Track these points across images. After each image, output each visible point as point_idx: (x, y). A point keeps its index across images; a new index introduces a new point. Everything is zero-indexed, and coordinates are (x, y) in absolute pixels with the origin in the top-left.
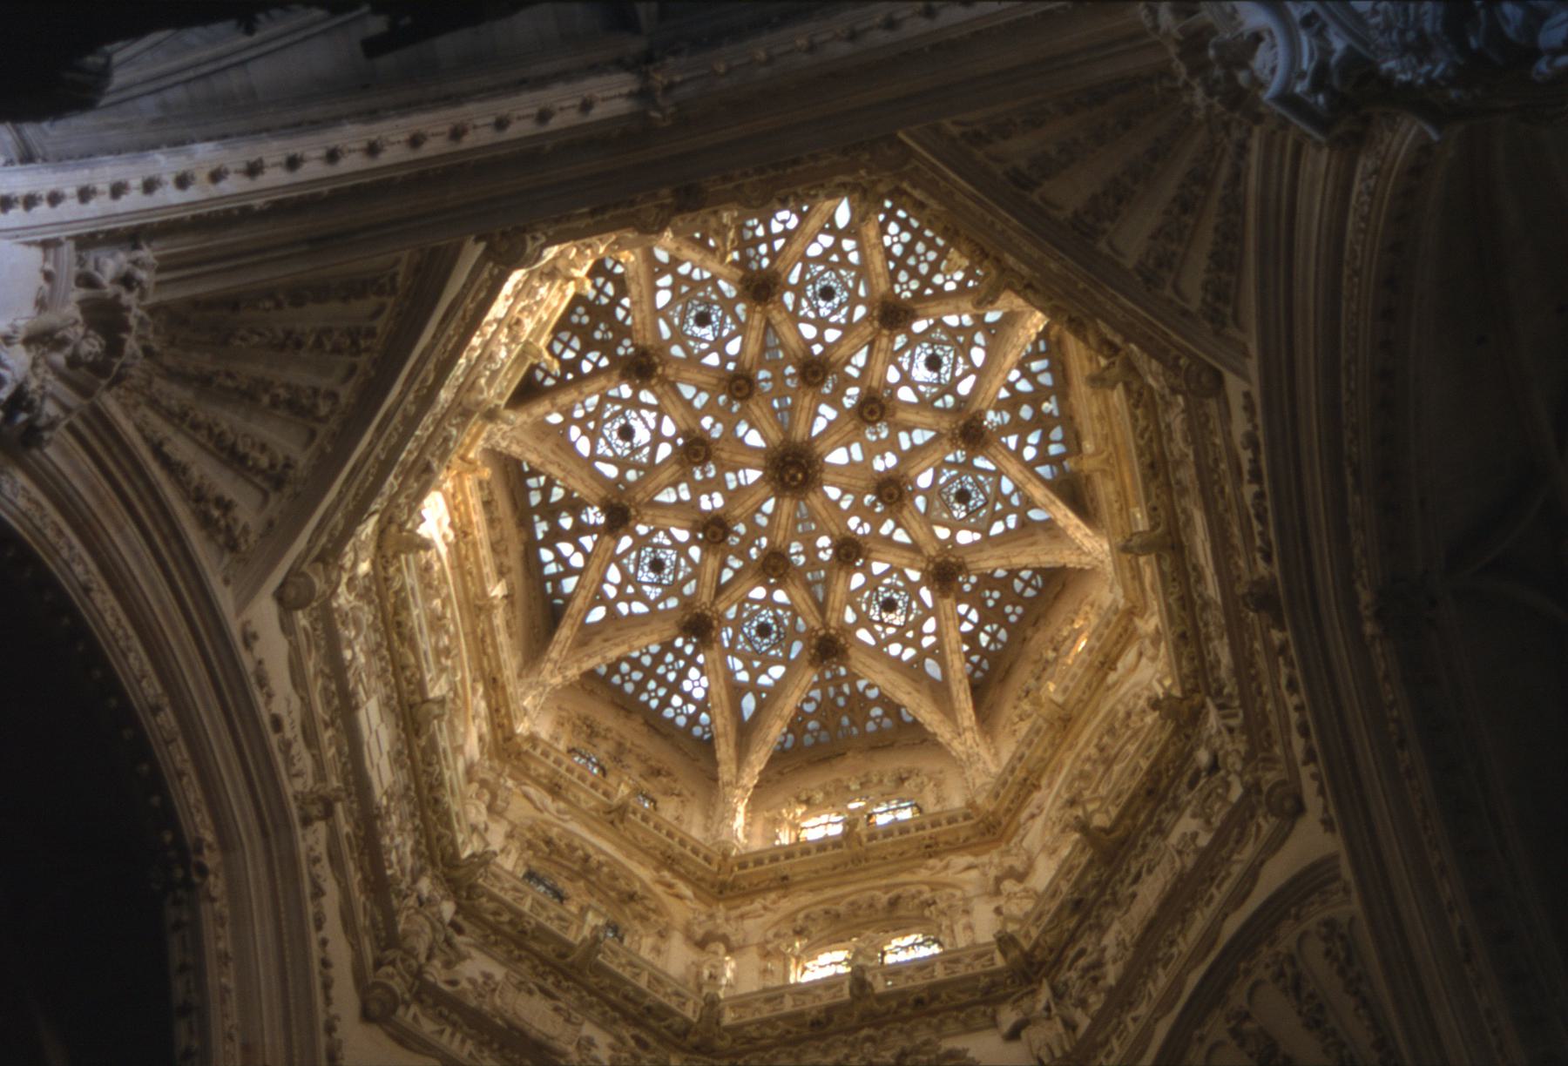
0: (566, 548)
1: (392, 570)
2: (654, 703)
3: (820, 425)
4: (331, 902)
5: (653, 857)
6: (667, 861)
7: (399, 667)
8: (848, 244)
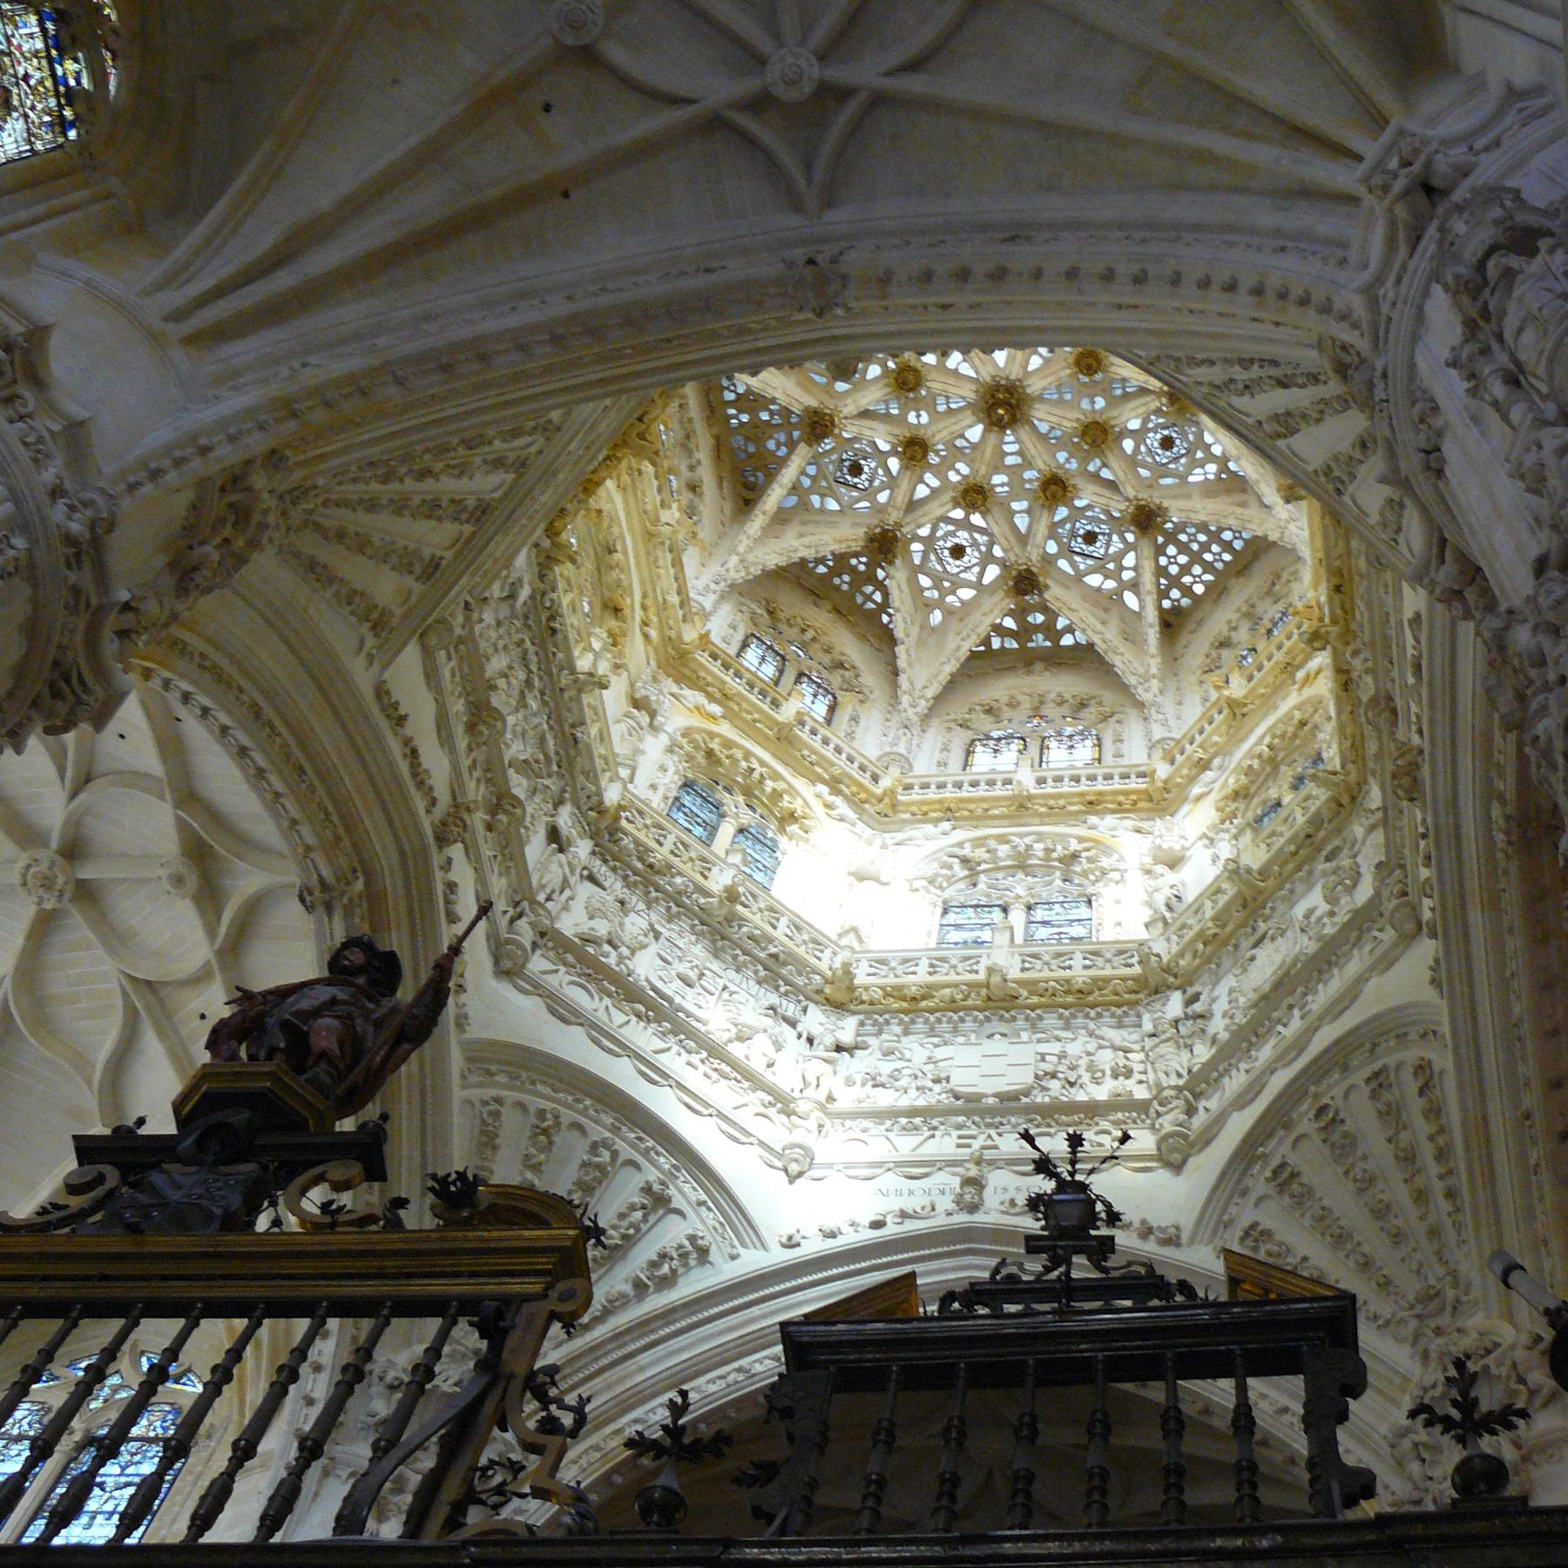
1: (865, 997)
2: (1227, 557)
5: (1283, 682)
7: (952, 1006)
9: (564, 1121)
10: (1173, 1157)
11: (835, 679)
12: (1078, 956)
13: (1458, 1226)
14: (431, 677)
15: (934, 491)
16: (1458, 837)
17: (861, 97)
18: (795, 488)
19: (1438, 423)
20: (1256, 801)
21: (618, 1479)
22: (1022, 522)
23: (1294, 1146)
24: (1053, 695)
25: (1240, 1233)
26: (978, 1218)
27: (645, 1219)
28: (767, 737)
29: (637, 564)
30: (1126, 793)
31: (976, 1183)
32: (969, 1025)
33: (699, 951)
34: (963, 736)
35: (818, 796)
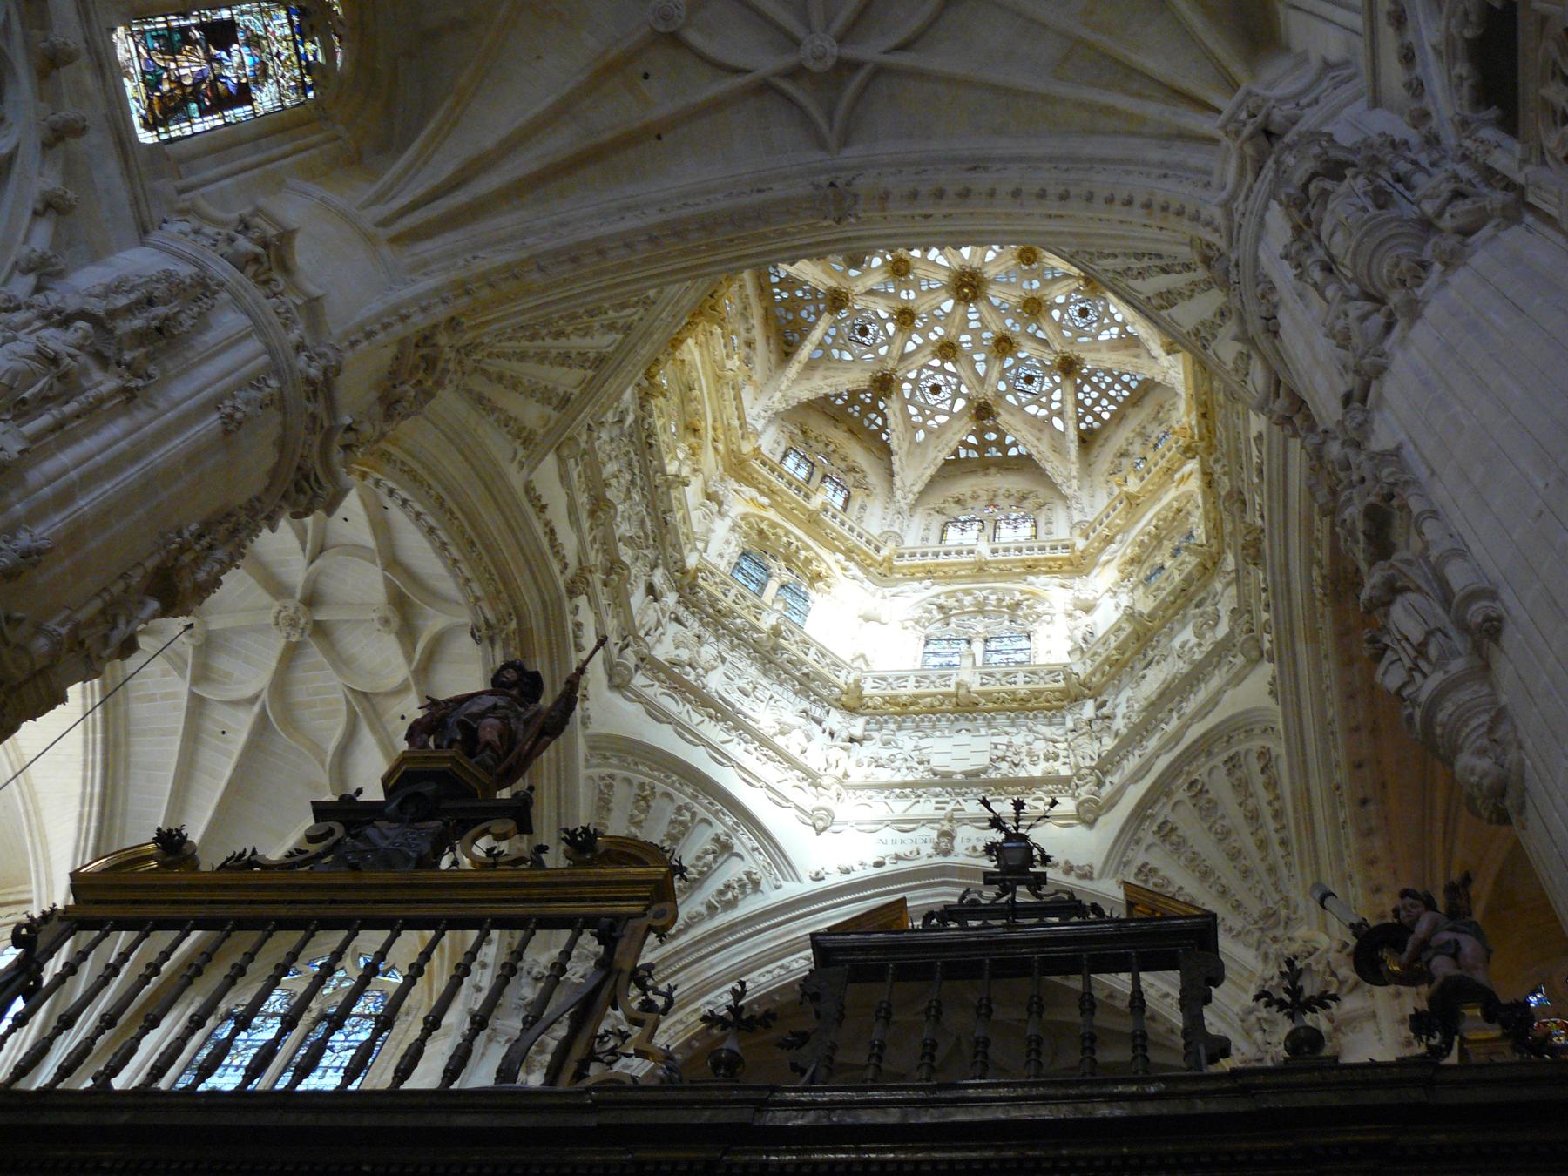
0: (1009, 440)
2: (1126, 393)
7: (932, 710)
9: (658, 791)
10: (1088, 815)
11: (849, 479)
12: (1021, 675)
13: (1289, 866)
14: (564, 478)
15: (919, 346)
16: (1289, 591)
17: (868, 69)
18: (821, 345)
19: (1275, 298)
20: (1146, 565)
21: (696, 1044)
22: (981, 369)
23: (1173, 808)
24: (1003, 491)
25: (1135, 870)
26: (950, 859)
27: (715, 860)
28: (801, 520)
29: (710, 398)
30: (1054, 560)
31: (948, 835)
32: (943, 723)
33: (753, 672)
34: (938, 520)
35: (837, 562)
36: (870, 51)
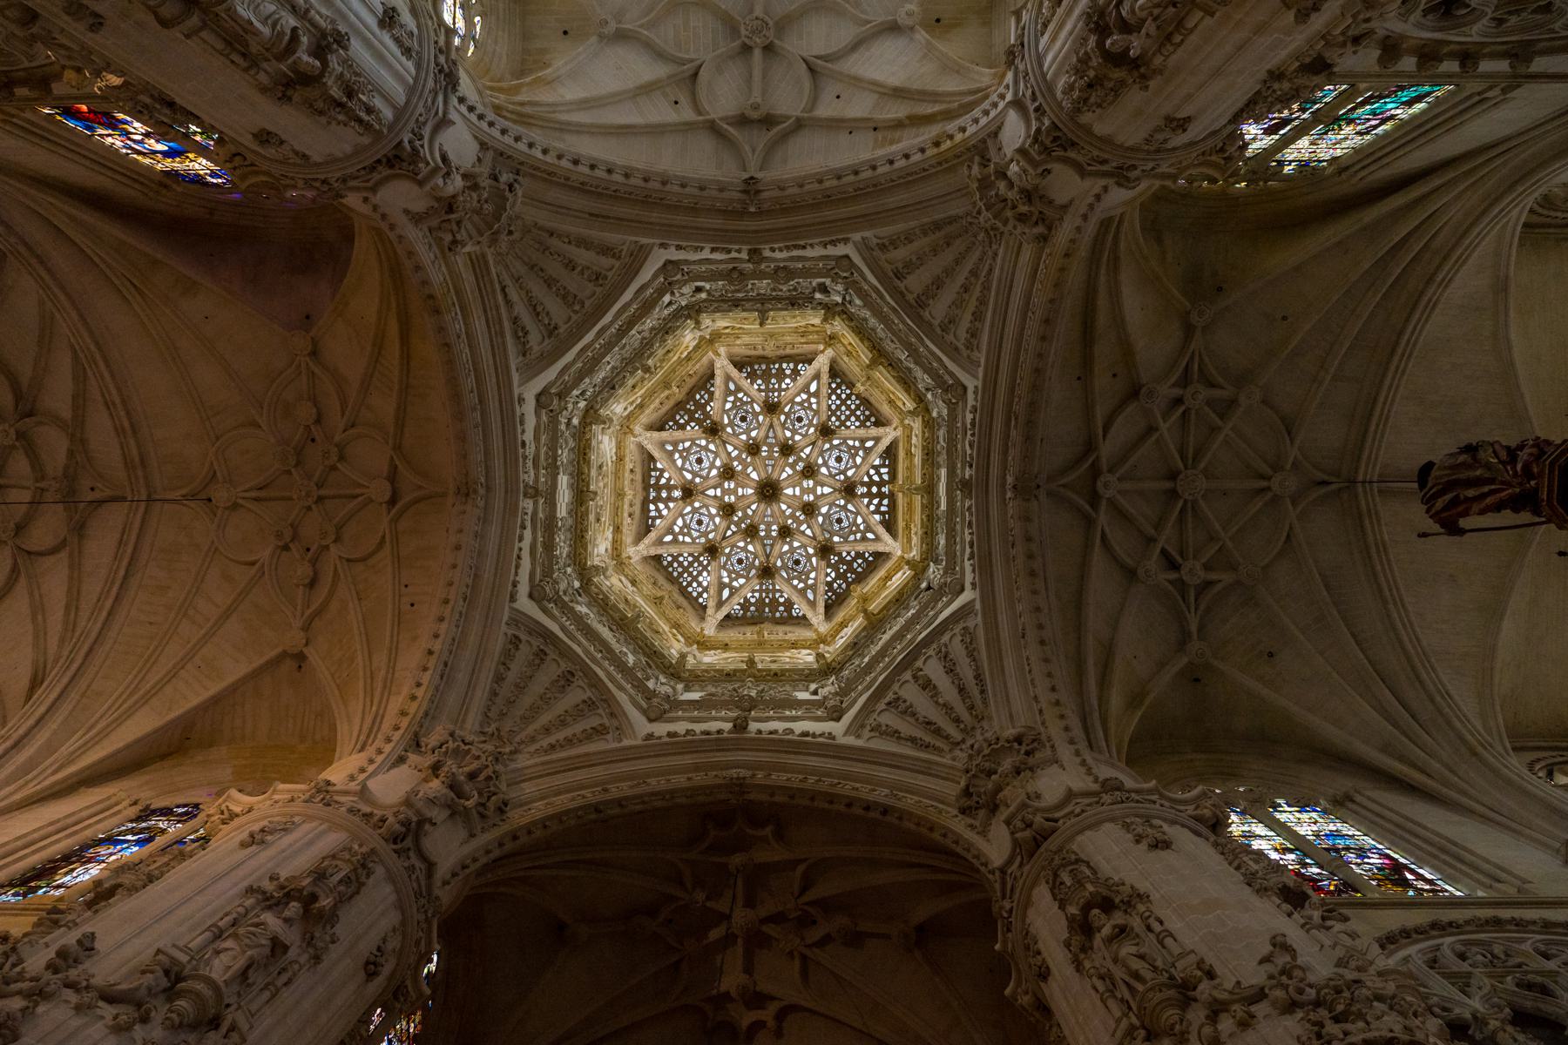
0: (661, 506)
3: (784, 475)
4: (526, 544)
6: (676, 626)
8: (813, 400)
17: (1094, 515)
36: (1103, 518)
